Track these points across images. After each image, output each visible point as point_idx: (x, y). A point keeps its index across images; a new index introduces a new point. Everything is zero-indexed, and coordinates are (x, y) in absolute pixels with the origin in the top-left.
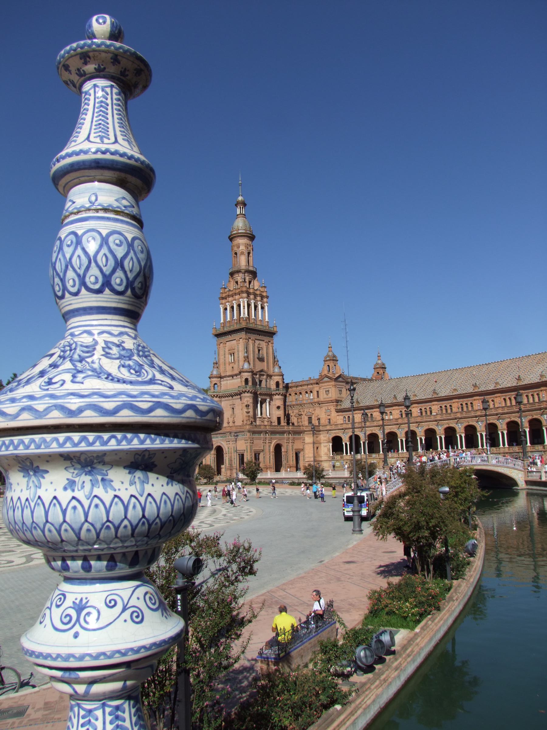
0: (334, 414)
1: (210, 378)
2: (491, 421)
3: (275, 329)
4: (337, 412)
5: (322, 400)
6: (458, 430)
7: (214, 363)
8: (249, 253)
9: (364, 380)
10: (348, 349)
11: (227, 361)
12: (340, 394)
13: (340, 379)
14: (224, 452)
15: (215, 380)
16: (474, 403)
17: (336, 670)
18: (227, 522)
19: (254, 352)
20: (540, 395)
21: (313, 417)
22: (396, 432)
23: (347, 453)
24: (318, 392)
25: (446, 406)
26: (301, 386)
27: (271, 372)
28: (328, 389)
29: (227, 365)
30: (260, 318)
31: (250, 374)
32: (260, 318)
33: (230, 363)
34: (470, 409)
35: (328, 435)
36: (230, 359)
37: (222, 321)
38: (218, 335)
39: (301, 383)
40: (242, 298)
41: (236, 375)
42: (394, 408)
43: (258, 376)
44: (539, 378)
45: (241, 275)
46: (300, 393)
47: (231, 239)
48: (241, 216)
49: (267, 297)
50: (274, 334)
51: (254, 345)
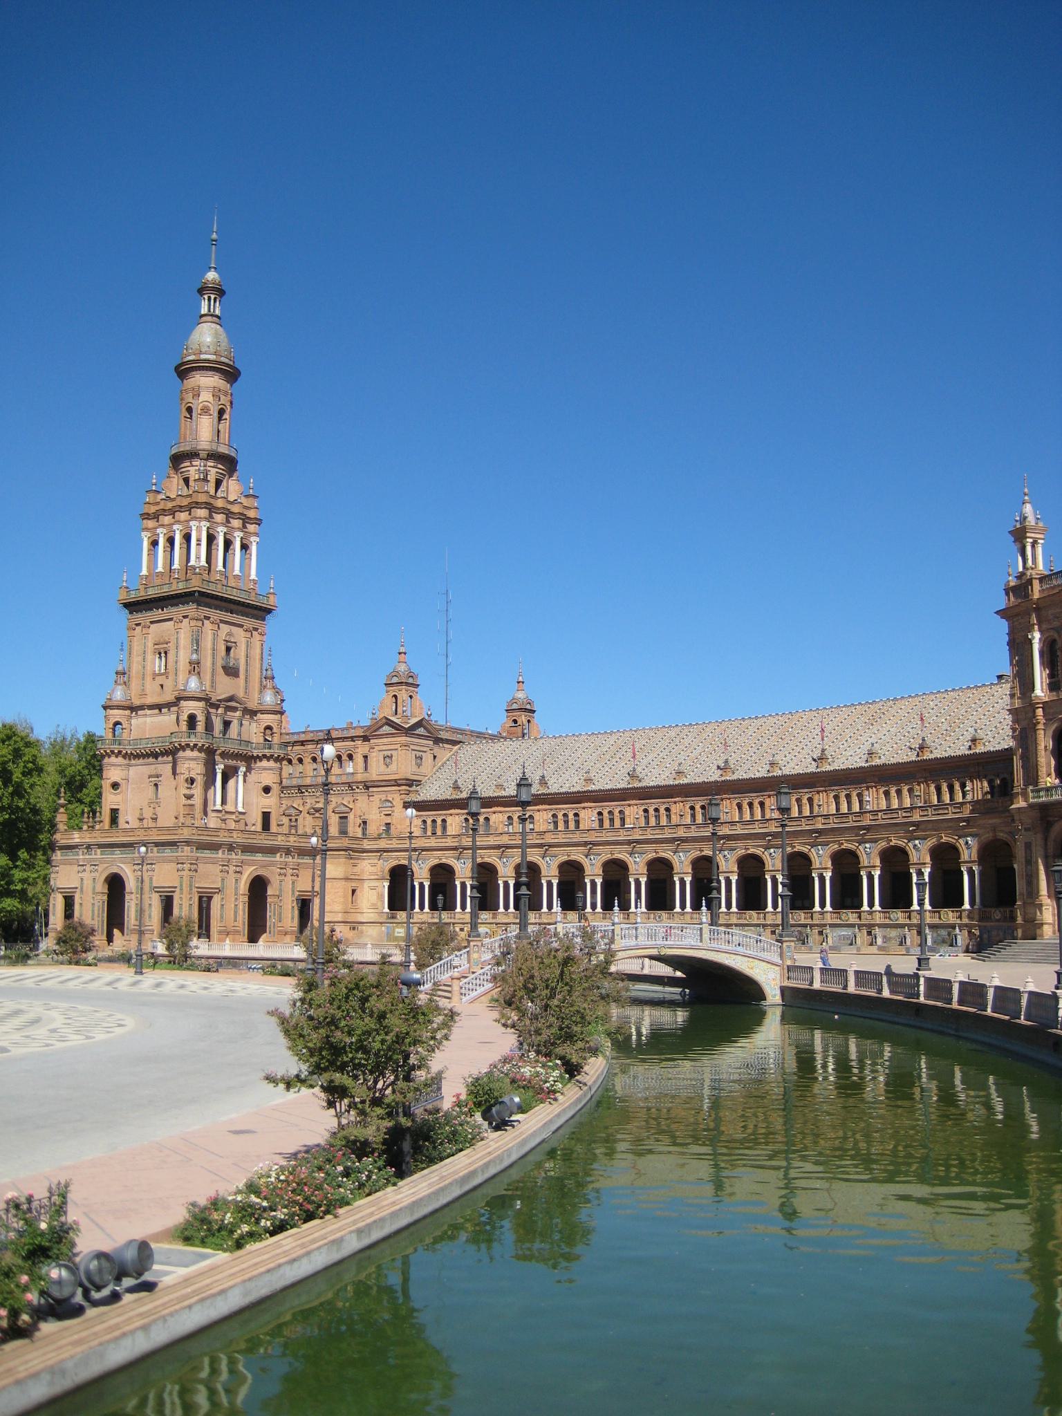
1: (105, 708)
2: (487, 860)
3: (272, 600)
5: (375, 777)
6: (632, 868)
8: (221, 412)
9: (480, 736)
11: (149, 668)
12: (419, 766)
13: (421, 731)
14: (127, 890)
15: (117, 715)
16: (627, 813)
17: (60, 1275)
18: (47, 1045)
20: (816, 802)
21: (351, 816)
24: (366, 757)
25: (565, 815)
27: (252, 705)
28: (389, 753)
29: (149, 679)
30: (237, 571)
31: (202, 704)
32: (237, 571)
33: (155, 676)
34: (664, 821)
36: (158, 665)
37: (144, 572)
38: (133, 606)
40: (195, 518)
41: (169, 705)
43: (220, 711)
44: (768, 767)
45: (197, 462)
46: (300, 761)
48: (209, 318)
49: (258, 522)
50: (269, 611)
51: (215, 636)
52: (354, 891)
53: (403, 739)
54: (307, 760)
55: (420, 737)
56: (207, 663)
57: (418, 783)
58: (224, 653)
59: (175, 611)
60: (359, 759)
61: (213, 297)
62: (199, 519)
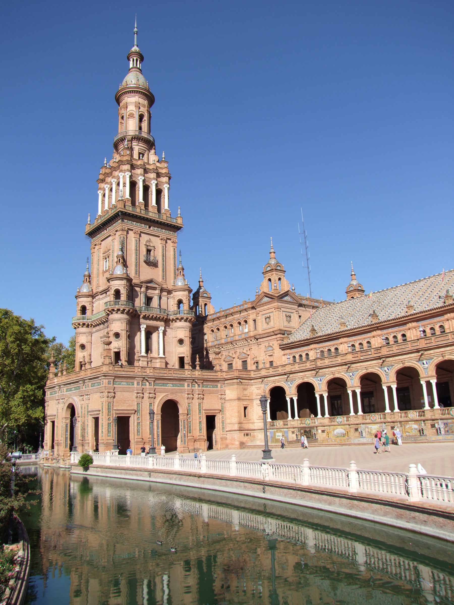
0: (278, 353)
3: (180, 221)
4: (283, 349)
5: (261, 332)
7: (84, 276)
8: (141, 117)
10: (310, 269)
12: (289, 322)
19: (138, 250)
21: (249, 361)
22: (379, 373)
23: (293, 416)
26: (232, 314)
27: (170, 287)
28: (268, 315)
31: (124, 282)
35: (263, 386)
39: (232, 311)
42: (374, 333)
43: (143, 289)
47: (118, 101)
48: (134, 69)
51: (138, 242)
52: (245, 408)
53: (276, 304)
54: (222, 328)
55: (287, 302)
56: (131, 260)
57: (290, 333)
58: (145, 253)
59: (110, 230)
60: (251, 322)
61: (135, 58)
62: (124, 171)
